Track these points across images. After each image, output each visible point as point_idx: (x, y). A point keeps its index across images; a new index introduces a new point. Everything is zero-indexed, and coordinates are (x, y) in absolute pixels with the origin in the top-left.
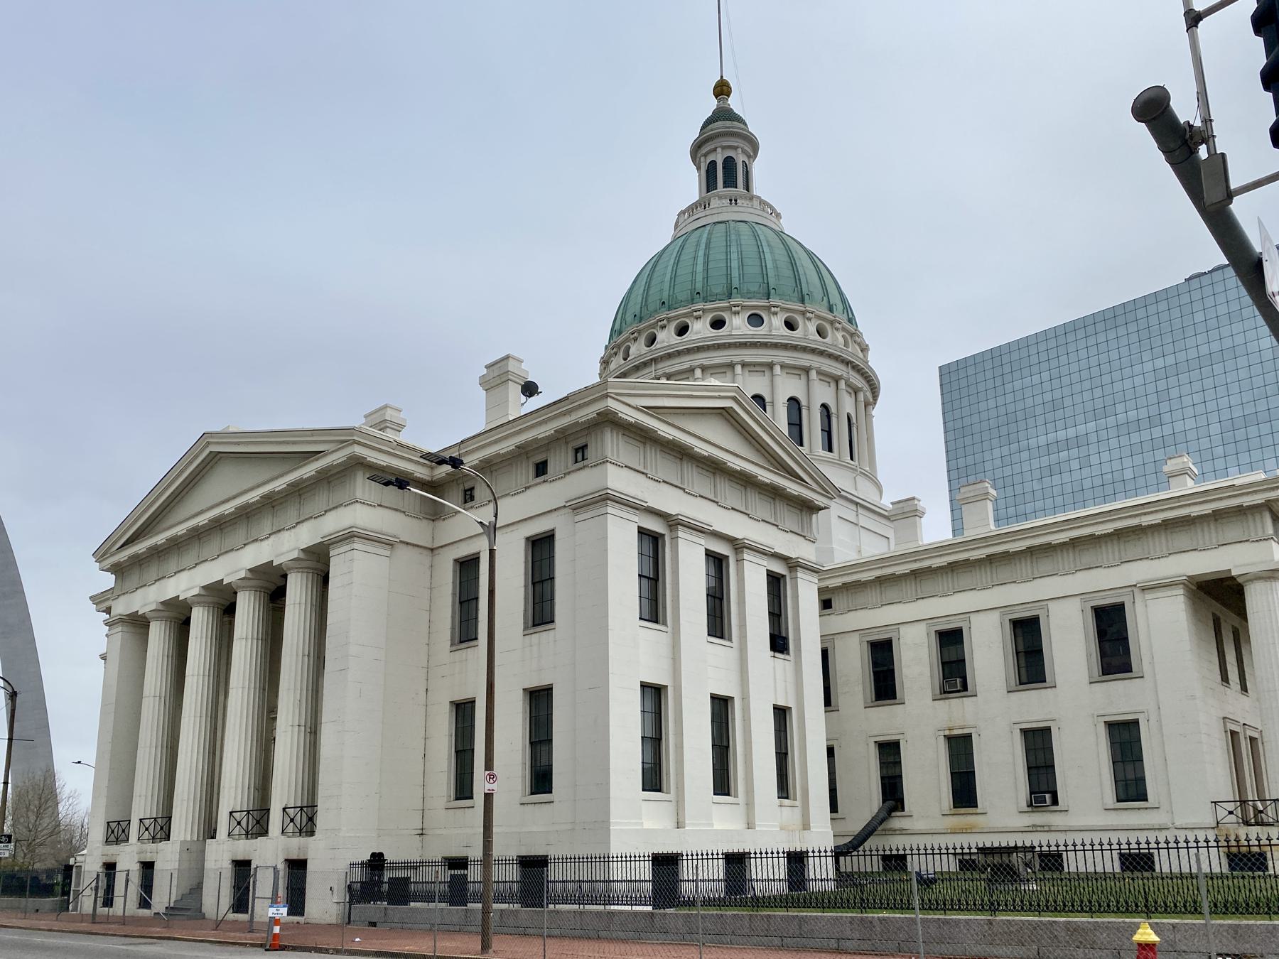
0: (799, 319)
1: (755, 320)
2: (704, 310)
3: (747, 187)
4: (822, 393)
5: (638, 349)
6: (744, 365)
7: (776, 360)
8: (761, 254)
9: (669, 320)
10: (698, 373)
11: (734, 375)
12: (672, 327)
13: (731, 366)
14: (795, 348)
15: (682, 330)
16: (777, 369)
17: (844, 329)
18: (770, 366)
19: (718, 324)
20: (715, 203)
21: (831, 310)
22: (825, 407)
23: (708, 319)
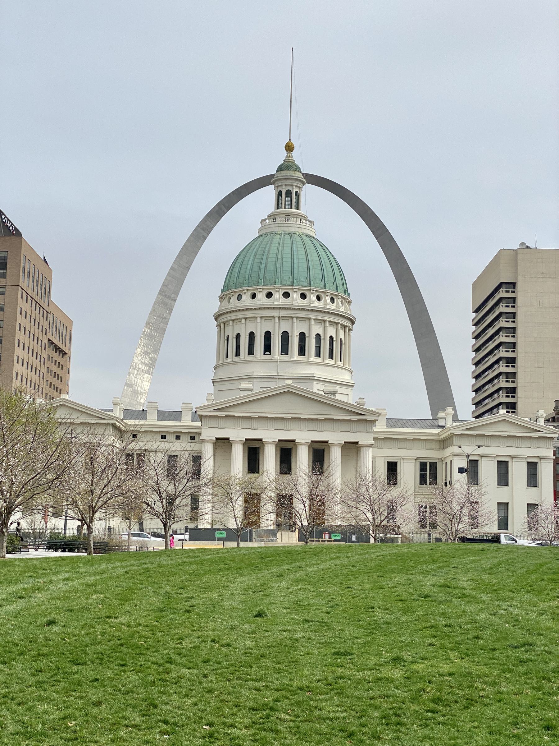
0: (307, 293)
1: (286, 295)
2: (263, 289)
3: (298, 208)
4: (317, 329)
5: (234, 303)
6: (279, 317)
7: (293, 316)
8: (292, 259)
9: (247, 290)
10: (259, 319)
11: (275, 322)
12: (249, 293)
13: (274, 317)
14: (304, 310)
15: (254, 296)
16: (295, 319)
17: (331, 294)
18: (292, 318)
19: (269, 295)
20: (278, 220)
21: (325, 286)
22: (318, 335)
23: (265, 292)
